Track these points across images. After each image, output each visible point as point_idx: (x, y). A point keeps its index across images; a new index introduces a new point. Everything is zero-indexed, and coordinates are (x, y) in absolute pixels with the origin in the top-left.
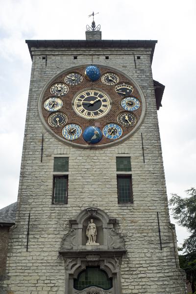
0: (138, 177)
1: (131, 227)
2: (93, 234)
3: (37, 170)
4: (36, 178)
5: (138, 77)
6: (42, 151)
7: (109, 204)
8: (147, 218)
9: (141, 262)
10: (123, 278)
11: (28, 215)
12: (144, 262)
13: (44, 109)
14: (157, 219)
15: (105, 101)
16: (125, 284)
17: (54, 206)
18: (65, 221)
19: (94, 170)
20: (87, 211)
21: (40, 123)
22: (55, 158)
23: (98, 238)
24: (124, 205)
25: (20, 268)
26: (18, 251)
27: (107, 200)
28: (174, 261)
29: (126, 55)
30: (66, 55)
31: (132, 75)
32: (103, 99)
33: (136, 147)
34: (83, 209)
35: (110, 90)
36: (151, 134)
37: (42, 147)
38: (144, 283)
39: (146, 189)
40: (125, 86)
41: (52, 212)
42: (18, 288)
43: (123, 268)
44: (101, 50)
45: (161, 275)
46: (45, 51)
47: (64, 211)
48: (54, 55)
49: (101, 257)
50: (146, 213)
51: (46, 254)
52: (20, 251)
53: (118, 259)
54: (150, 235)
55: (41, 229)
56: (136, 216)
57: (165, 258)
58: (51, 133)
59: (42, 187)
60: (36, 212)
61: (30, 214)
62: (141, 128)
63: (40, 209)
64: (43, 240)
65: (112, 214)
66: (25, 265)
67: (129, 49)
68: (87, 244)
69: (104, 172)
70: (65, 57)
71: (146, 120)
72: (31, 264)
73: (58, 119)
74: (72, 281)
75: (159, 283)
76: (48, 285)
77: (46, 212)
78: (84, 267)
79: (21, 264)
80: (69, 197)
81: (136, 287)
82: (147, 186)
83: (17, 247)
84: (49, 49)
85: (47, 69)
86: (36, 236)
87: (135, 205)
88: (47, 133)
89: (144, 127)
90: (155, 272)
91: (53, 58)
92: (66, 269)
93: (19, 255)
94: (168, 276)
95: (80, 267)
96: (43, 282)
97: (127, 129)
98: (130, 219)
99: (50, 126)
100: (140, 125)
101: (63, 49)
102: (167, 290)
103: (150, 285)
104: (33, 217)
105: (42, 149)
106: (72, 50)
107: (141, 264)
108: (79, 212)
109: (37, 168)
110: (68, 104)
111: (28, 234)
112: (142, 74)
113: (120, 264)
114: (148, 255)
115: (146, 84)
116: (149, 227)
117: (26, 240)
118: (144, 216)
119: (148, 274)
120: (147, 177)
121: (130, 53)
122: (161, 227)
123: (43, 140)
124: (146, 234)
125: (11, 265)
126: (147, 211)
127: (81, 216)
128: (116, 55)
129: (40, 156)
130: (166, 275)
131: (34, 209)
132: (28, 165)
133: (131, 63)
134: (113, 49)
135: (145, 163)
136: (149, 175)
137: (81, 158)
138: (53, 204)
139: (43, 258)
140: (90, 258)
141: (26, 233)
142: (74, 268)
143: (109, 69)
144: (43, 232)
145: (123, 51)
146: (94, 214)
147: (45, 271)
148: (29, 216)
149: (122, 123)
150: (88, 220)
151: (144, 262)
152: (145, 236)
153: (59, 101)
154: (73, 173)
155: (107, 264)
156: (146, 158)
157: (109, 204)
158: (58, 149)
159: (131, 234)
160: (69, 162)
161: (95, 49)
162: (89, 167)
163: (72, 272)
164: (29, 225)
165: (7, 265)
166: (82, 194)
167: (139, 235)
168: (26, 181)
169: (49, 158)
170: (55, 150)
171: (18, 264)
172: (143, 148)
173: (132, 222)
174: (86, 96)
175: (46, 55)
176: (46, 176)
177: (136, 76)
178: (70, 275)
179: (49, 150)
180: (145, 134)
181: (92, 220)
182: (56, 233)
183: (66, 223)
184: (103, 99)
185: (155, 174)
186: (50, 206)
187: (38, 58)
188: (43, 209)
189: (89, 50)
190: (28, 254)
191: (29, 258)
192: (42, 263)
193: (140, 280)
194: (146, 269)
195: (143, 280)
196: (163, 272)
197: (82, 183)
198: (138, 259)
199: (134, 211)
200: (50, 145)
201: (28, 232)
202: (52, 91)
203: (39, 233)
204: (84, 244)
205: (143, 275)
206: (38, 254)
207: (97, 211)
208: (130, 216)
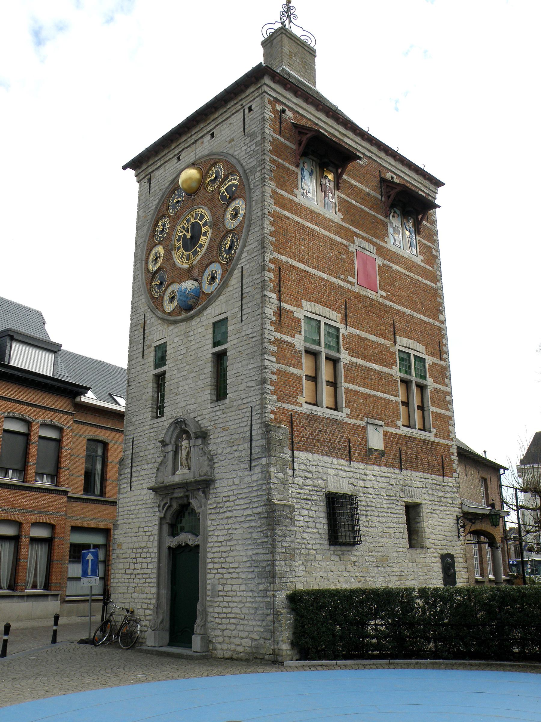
0: (233, 351)
3: (140, 372)
4: (138, 385)
8: (240, 420)
10: (210, 520)
12: (231, 493)
15: (205, 224)
19: (190, 354)
22: (156, 347)
27: (199, 401)
29: (233, 114)
30: (169, 160)
36: (254, 263)
39: (241, 369)
41: (152, 430)
42: (125, 539)
43: (210, 504)
44: (202, 126)
45: (249, 512)
48: (157, 169)
49: (188, 491)
50: (239, 412)
53: (204, 492)
54: (241, 447)
56: (227, 419)
57: (255, 484)
60: (140, 434)
62: (244, 255)
64: (143, 473)
65: (204, 421)
66: (129, 508)
67: (235, 102)
68: (177, 473)
69: (200, 355)
70: (168, 166)
71: (250, 238)
72: (133, 508)
74: (165, 528)
75: (247, 525)
77: (146, 432)
78: (175, 506)
81: (223, 533)
82: (244, 363)
84: (150, 163)
85: (151, 199)
87: (227, 401)
91: (157, 173)
93: (125, 496)
95: (170, 506)
98: (221, 425)
100: (242, 252)
101: (164, 153)
102: (254, 535)
103: (236, 529)
105: (144, 338)
106: (173, 147)
107: (229, 496)
109: (139, 369)
111: (132, 467)
113: (207, 499)
114: (237, 481)
115: (255, 163)
118: (236, 417)
119: (235, 512)
120: (244, 348)
121: (238, 107)
124: (235, 448)
126: (241, 407)
127: (170, 433)
128: (222, 122)
130: (255, 511)
131: (137, 431)
132: (133, 367)
135: (244, 322)
136: (247, 342)
137: (177, 340)
139: (142, 497)
141: (130, 465)
142: (165, 510)
144: (144, 462)
145: (229, 108)
148: (133, 442)
150: (179, 437)
151: (231, 493)
152: (236, 451)
156: (244, 312)
160: (168, 348)
162: (184, 351)
166: (176, 397)
167: (228, 450)
169: (150, 349)
171: (125, 508)
172: (242, 295)
173: (224, 430)
176: (146, 378)
180: (247, 266)
185: (254, 339)
187: (143, 183)
190: (132, 492)
192: (142, 504)
193: (225, 521)
195: (230, 521)
197: (176, 381)
198: (226, 489)
199: (227, 410)
203: (140, 463)
204: (174, 474)
205: (229, 514)
206: (139, 492)
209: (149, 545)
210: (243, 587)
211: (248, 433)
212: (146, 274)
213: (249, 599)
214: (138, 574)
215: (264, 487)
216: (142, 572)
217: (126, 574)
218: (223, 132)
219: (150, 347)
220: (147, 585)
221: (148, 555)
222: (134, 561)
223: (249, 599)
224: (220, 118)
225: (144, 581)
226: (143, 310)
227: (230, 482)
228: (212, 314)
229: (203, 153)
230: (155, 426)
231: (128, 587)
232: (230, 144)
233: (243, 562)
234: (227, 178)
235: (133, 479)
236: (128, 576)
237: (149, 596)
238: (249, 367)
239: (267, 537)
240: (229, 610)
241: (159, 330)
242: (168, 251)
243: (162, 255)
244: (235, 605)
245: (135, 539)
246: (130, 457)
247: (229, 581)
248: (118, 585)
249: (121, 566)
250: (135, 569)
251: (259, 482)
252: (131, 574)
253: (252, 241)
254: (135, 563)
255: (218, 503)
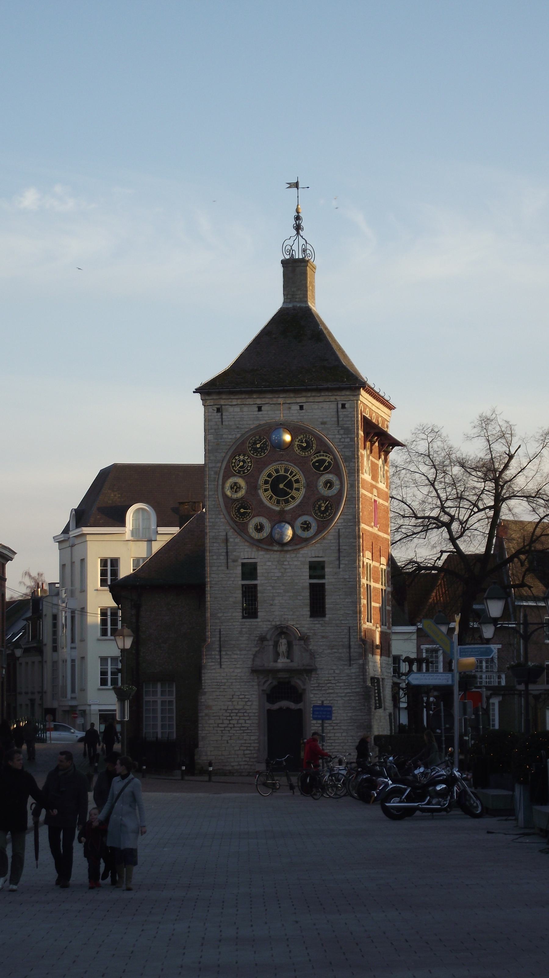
1: (322, 643)
2: (285, 651)
4: (223, 588)
5: (340, 442)
6: (227, 555)
7: (300, 619)
9: (330, 678)
11: (218, 630)
13: (225, 495)
14: (348, 634)
15: (297, 481)
16: (314, 699)
17: (244, 620)
18: (256, 637)
19: (285, 578)
20: (276, 627)
21: (222, 516)
23: (289, 654)
24: (315, 619)
25: (216, 684)
26: (212, 668)
28: (361, 677)
31: (333, 438)
32: (295, 478)
33: (332, 548)
34: (273, 623)
35: (301, 463)
37: (227, 549)
38: (331, 698)
40: (323, 456)
41: (243, 627)
45: (348, 691)
46: (220, 399)
47: (254, 627)
51: (239, 670)
52: (214, 667)
53: (307, 676)
54: (340, 651)
55: (232, 646)
58: (236, 531)
59: (231, 599)
61: (220, 629)
63: (230, 624)
64: (236, 656)
65: (303, 629)
66: (220, 681)
68: (279, 661)
70: (245, 409)
72: (225, 681)
73: (242, 510)
76: (243, 700)
78: (275, 683)
79: (215, 681)
80: (259, 610)
83: (211, 664)
85: (224, 431)
86: (228, 653)
87: (327, 619)
88: (232, 530)
89: (342, 521)
90: (342, 688)
91: (231, 409)
92: (259, 685)
93: (214, 671)
94: (355, 692)
95: (271, 683)
96: (238, 697)
97: (323, 526)
99: (232, 518)
101: (243, 396)
104: (224, 633)
105: (227, 552)
108: (269, 627)
109: (223, 576)
110: (253, 488)
111: (220, 651)
112: (346, 436)
113: (310, 680)
114: (337, 672)
116: (341, 643)
117: (218, 657)
121: (333, 398)
122: (352, 643)
123: (227, 540)
124: (335, 651)
125: (207, 681)
129: (225, 561)
130: (353, 690)
133: (333, 417)
134: (309, 395)
135: (341, 569)
137: (269, 564)
138: (244, 617)
139: (235, 674)
140: (281, 675)
141: (218, 649)
143: (303, 429)
146: (285, 630)
147: (239, 687)
149: (317, 514)
151: (333, 678)
153: (242, 482)
154: (262, 582)
155: (297, 682)
156: (342, 562)
157: (300, 619)
158: (245, 553)
159: (321, 651)
160: (258, 568)
161: (284, 396)
162: (280, 574)
163: (265, 687)
164: (220, 641)
165: (203, 682)
166: (273, 607)
167: (329, 651)
168: (213, 592)
169: (236, 564)
170: (242, 553)
172: (339, 549)
173: (323, 637)
174: (275, 474)
175: (221, 405)
177: (338, 440)
178: (263, 690)
179: (234, 553)
180: (344, 530)
181: (283, 636)
182: (247, 649)
183: (257, 638)
184: (295, 478)
185: (350, 583)
186: (240, 620)
187: (211, 410)
188: (234, 624)
189: (277, 396)
191: (223, 675)
194: (334, 685)
195: (332, 695)
196: (350, 687)
197: (271, 595)
198: (327, 675)
200: (237, 547)
201: (220, 648)
202: (233, 467)
204: (276, 661)
206: (232, 670)
207: (287, 627)
208: (321, 631)
209: (246, 707)
210: (344, 734)
211: (347, 643)
212: (223, 498)
213: (350, 741)
214: (234, 727)
215: (361, 677)
216: (240, 725)
217: (218, 727)
218: (314, 411)
219: (234, 561)
220: (245, 734)
221: (245, 714)
222: (230, 718)
223: (350, 741)
224: (311, 398)
225: (242, 732)
226: (223, 527)
227: (332, 672)
228: (310, 553)
229: (291, 418)
230: (246, 623)
231: (222, 736)
232: (323, 426)
233: (344, 720)
234: (319, 452)
235: (223, 660)
236: (223, 729)
237: (247, 742)
238: (347, 600)
239: (364, 706)
240: (333, 747)
241: (246, 550)
242: (253, 488)
243: (244, 488)
244: (337, 744)
245: (230, 703)
246: (217, 643)
247: (332, 731)
248: (208, 735)
249: (211, 721)
250: (230, 724)
251: (357, 674)
252: (225, 727)
253: (348, 514)
254: (230, 720)
255: (319, 684)
